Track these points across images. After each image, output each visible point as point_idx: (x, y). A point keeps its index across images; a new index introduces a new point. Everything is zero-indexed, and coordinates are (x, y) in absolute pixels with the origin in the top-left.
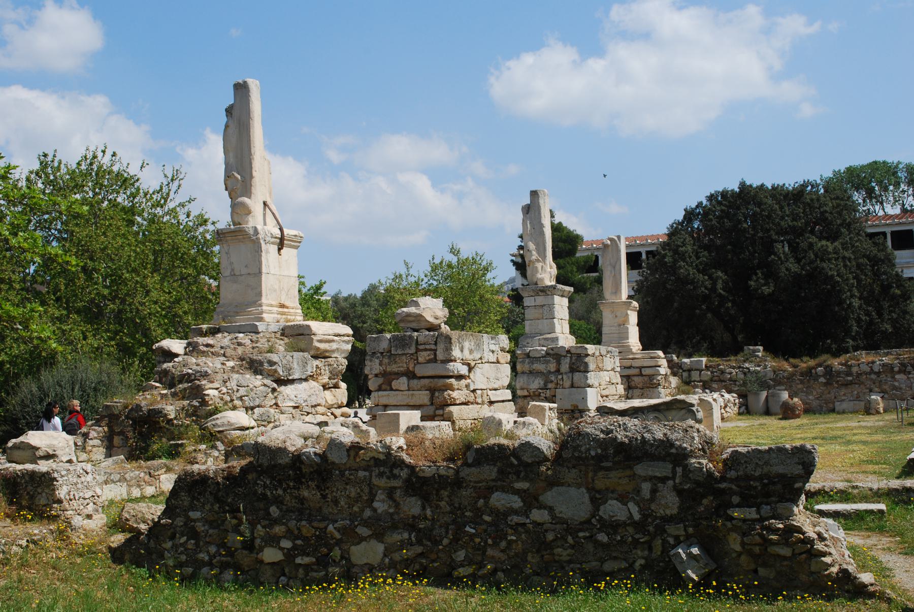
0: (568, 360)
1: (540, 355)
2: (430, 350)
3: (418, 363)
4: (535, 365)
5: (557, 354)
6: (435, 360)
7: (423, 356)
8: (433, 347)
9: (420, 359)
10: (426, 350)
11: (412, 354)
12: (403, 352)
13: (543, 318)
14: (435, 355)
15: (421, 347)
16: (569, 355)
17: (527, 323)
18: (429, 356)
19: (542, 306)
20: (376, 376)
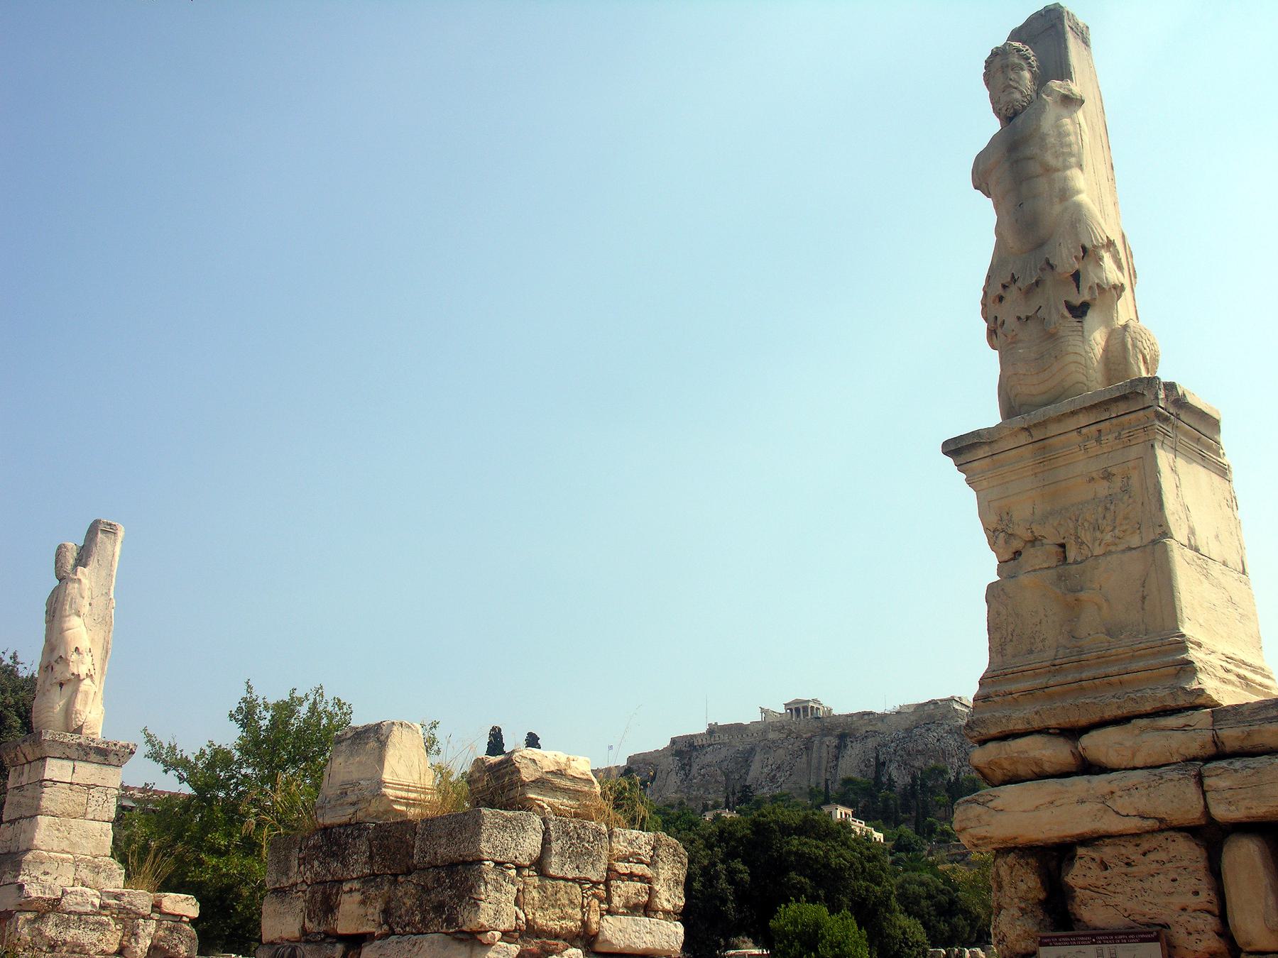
0: (152, 925)
1: (89, 908)
2: (642, 878)
3: (609, 912)
4: (73, 932)
5: (128, 912)
6: (647, 909)
7: (625, 891)
8: (648, 872)
9: (617, 901)
10: (631, 876)
11: (595, 884)
12: (576, 874)
13: (84, 815)
14: (652, 893)
15: (622, 867)
16: (156, 916)
17: (43, 821)
18: (638, 894)
19: (89, 787)
20: (507, 936)
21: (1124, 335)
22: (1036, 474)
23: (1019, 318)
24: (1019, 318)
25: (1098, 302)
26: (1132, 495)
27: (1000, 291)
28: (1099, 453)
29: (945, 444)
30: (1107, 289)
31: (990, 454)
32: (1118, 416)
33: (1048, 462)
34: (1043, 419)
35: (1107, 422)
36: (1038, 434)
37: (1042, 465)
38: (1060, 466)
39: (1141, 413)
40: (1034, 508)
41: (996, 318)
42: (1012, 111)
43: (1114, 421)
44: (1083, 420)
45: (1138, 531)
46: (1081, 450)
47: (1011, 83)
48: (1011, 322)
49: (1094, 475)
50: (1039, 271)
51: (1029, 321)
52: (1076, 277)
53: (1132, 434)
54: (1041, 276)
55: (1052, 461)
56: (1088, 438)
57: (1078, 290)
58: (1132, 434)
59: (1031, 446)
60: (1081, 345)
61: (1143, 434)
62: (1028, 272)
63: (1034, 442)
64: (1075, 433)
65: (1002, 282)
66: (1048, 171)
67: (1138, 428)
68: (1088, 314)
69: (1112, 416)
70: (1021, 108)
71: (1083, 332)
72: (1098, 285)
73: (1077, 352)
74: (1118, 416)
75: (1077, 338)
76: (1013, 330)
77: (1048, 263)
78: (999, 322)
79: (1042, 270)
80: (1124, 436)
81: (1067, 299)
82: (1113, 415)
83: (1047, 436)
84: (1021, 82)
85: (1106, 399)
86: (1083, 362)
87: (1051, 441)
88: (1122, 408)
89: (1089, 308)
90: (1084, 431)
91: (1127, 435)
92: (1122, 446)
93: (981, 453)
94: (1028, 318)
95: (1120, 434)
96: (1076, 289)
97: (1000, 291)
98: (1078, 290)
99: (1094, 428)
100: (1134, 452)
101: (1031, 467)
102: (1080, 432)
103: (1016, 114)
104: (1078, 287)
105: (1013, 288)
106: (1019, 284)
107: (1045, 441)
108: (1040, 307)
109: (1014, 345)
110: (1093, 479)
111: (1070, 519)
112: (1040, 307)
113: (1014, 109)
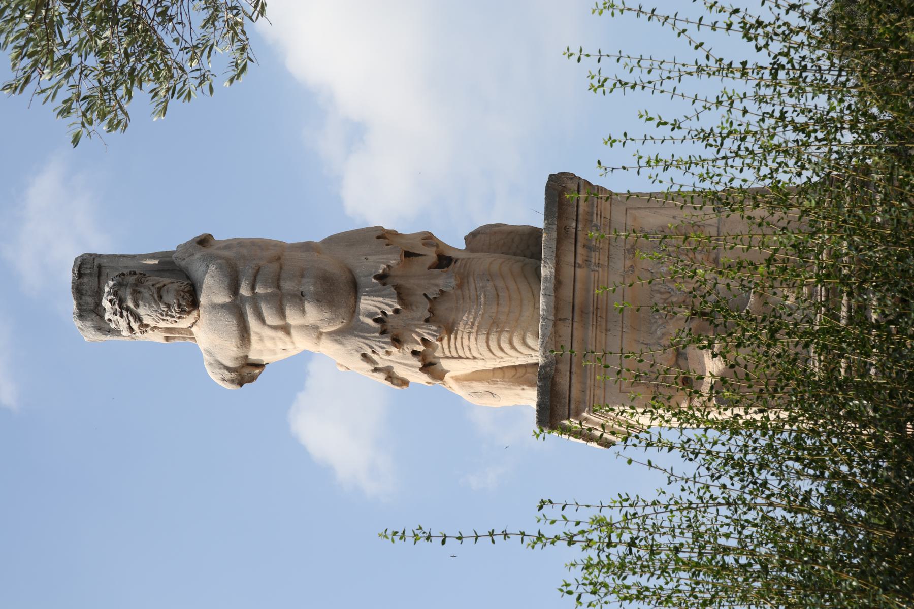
22: (607, 330)
23: (427, 321)
26: (661, 229)
28: (607, 255)
31: (568, 373)
32: (577, 220)
33: (599, 310)
37: (599, 319)
38: (607, 301)
40: (642, 343)
42: (188, 295)
43: (580, 227)
45: (702, 227)
46: (598, 271)
47: (158, 286)
49: (628, 263)
51: (434, 312)
52: (408, 255)
53: (599, 213)
55: (599, 306)
56: (587, 261)
58: (599, 213)
59: (575, 325)
63: (573, 319)
64: (578, 271)
66: (279, 258)
67: (595, 203)
74: (577, 220)
80: (599, 221)
81: (427, 266)
82: (574, 225)
83: (571, 301)
87: (577, 301)
89: (443, 256)
90: (579, 261)
91: (599, 216)
92: (608, 228)
93: (563, 382)
94: (431, 311)
95: (596, 226)
99: (580, 250)
100: (618, 217)
101: (598, 332)
104: (419, 255)
107: (576, 308)
108: (425, 295)
110: (631, 266)
111: (667, 299)
112: (425, 295)
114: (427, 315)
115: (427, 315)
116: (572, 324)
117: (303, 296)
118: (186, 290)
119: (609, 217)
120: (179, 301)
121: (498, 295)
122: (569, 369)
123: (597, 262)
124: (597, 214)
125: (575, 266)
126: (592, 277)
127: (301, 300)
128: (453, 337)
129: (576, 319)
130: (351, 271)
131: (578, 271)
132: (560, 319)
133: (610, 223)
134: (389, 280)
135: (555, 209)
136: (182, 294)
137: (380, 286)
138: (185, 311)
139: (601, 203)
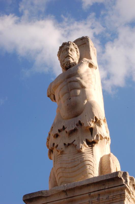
21: (109, 159)
23: (65, 144)
24: (65, 144)
25: (99, 142)
27: (57, 132)
29: (25, 196)
30: (103, 138)
32: (108, 188)
34: (73, 187)
35: (103, 191)
36: (70, 195)
39: (120, 187)
41: (54, 144)
42: (69, 65)
44: (92, 189)
46: (90, 203)
48: (61, 146)
50: (76, 125)
51: (69, 146)
53: (114, 197)
54: (77, 128)
57: (92, 135)
58: (114, 197)
59: (66, 200)
60: (92, 157)
61: (120, 197)
62: (71, 125)
65: (58, 128)
68: (95, 146)
69: (106, 188)
70: (72, 65)
71: (93, 153)
72: (101, 135)
73: (90, 160)
74: (108, 188)
75: (90, 155)
76: (62, 149)
77: (80, 122)
78: (55, 146)
79: (77, 125)
81: (87, 138)
82: (106, 187)
83: (75, 195)
84: (73, 56)
85: (104, 179)
86: (93, 165)
87: (74, 198)
88: (112, 185)
90: (92, 194)
91: (112, 197)
94: (69, 144)
95: (108, 197)
96: (91, 135)
97: (57, 132)
98: (92, 135)
102: (90, 195)
103: (70, 67)
105: (64, 132)
106: (67, 130)
108: (75, 140)
109: (61, 155)
112: (75, 140)
113: (70, 65)
114: (67, 144)
115: (67, 144)
116: (66, 198)
117: (69, 99)
118: (70, 64)
119: (113, 202)
120: (66, 63)
121: (76, 166)
122: (48, 202)
123: (93, 202)
124: (113, 196)
125: (89, 193)
126: (87, 201)
127: (68, 99)
128: (60, 156)
129: (68, 199)
130: (82, 112)
131: (88, 195)
132: (66, 193)
133: (112, 203)
134: (79, 126)
135: (110, 177)
136: (68, 63)
137: (76, 123)
138: (63, 66)
139: (119, 197)
